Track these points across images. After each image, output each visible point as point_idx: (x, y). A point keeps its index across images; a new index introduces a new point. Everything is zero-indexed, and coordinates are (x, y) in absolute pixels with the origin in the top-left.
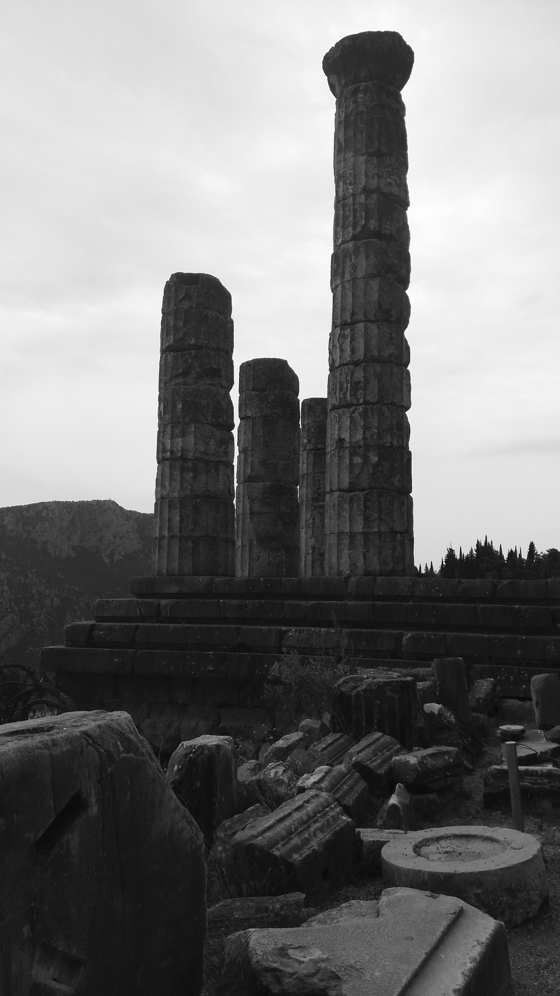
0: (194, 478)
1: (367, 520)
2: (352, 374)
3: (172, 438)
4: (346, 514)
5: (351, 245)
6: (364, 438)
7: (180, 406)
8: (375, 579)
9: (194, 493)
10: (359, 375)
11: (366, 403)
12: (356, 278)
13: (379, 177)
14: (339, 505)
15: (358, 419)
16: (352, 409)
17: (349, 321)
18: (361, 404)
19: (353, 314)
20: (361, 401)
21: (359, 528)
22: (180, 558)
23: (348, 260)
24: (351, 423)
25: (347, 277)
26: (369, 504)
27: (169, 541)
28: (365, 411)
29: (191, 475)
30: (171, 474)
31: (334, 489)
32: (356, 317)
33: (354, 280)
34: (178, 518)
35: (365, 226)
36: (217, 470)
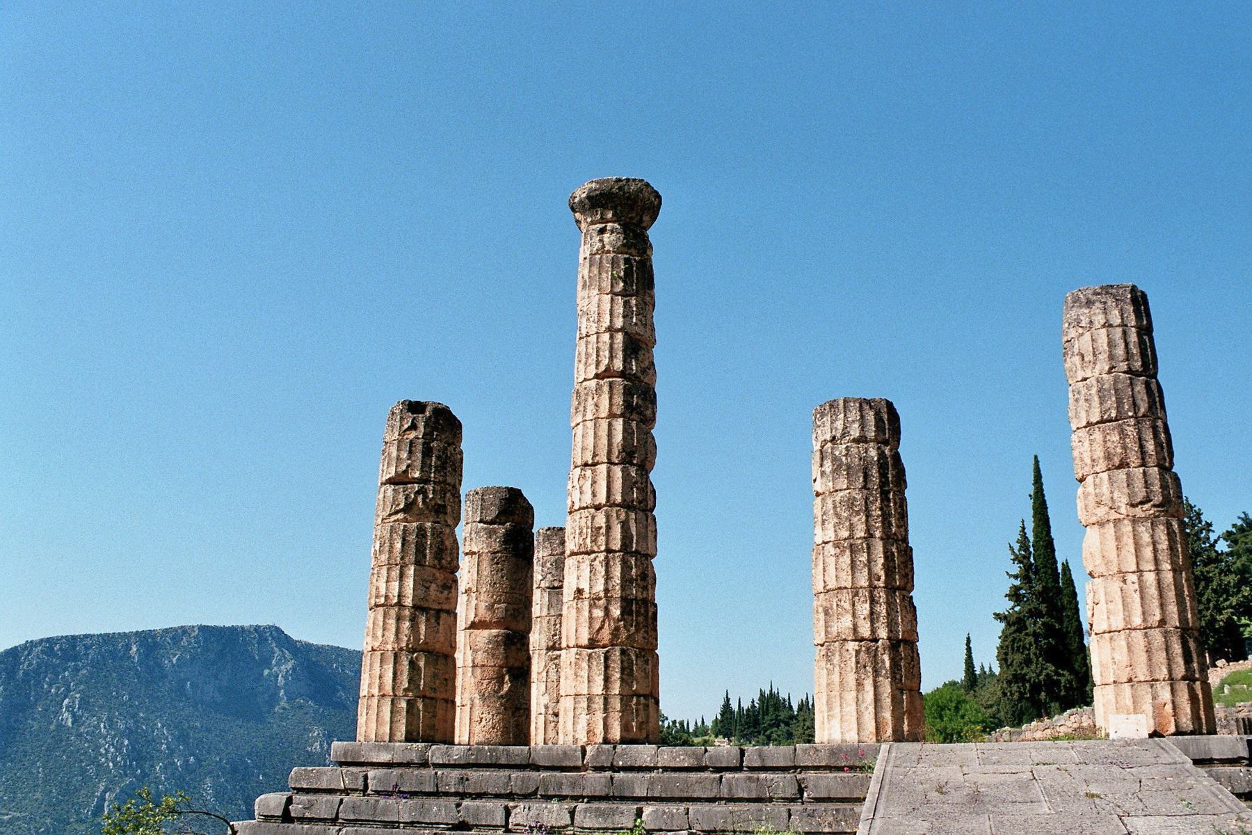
2: (593, 518)
4: (584, 673)
5: (593, 383)
6: (606, 590)
8: (615, 748)
10: (601, 520)
11: (608, 551)
16: (593, 556)
17: (590, 462)
19: (595, 455)
28: (606, 557)
36: (438, 618)
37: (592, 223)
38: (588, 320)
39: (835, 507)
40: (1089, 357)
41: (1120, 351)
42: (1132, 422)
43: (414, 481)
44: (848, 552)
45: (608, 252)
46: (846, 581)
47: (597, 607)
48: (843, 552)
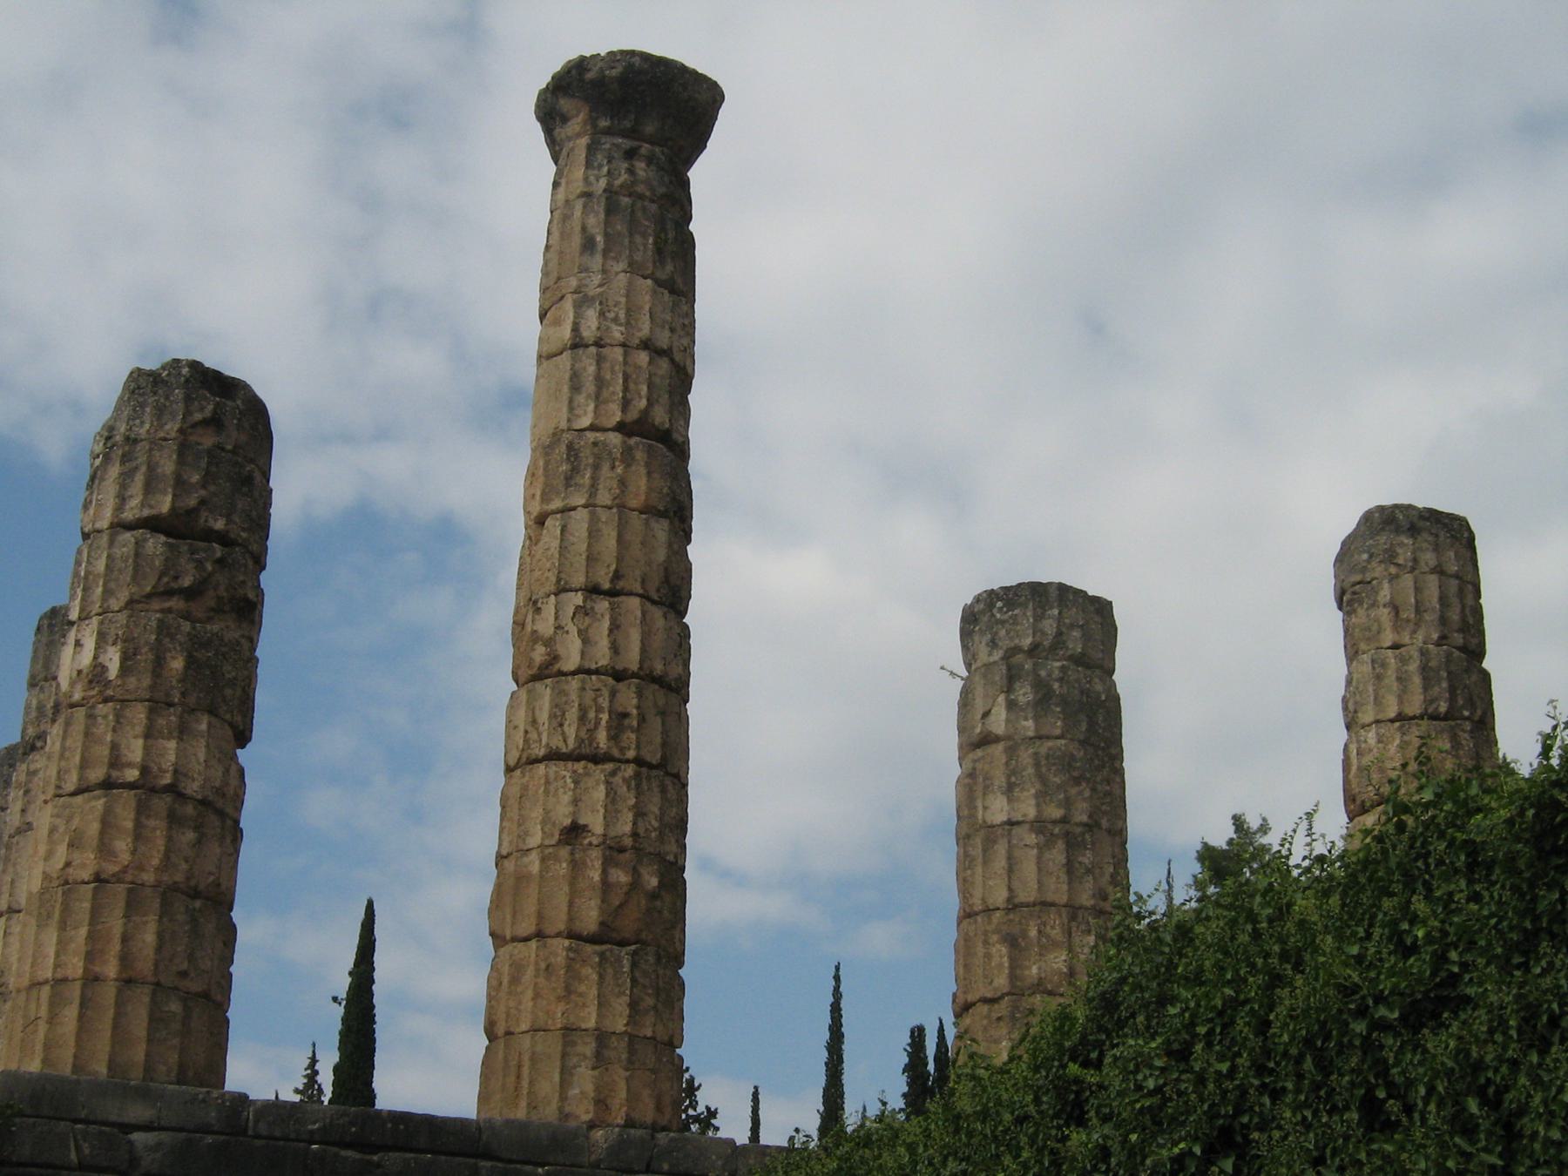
0: (199, 842)
3: (147, 736)
6: (635, 835)
7: (177, 664)
9: (193, 883)
13: (672, 330)
14: (569, 968)
16: (609, 766)
17: (606, 586)
18: (628, 761)
19: (617, 576)
20: (631, 754)
21: (620, 1025)
22: (150, 1041)
24: (607, 795)
25: (604, 497)
26: (637, 974)
27: (120, 992)
28: (637, 775)
29: (190, 836)
30: (138, 825)
31: (550, 929)
35: (646, 413)
37: (608, 132)
38: (602, 314)
39: (1037, 765)
40: (1408, 613)
41: (1454, 616)
42: (1468, 726)
43: (209, 535)
44: (1061, 845)
45: (641, 197)
46: (1058, 891)
47: (617, 865)
48: (1048, 844)
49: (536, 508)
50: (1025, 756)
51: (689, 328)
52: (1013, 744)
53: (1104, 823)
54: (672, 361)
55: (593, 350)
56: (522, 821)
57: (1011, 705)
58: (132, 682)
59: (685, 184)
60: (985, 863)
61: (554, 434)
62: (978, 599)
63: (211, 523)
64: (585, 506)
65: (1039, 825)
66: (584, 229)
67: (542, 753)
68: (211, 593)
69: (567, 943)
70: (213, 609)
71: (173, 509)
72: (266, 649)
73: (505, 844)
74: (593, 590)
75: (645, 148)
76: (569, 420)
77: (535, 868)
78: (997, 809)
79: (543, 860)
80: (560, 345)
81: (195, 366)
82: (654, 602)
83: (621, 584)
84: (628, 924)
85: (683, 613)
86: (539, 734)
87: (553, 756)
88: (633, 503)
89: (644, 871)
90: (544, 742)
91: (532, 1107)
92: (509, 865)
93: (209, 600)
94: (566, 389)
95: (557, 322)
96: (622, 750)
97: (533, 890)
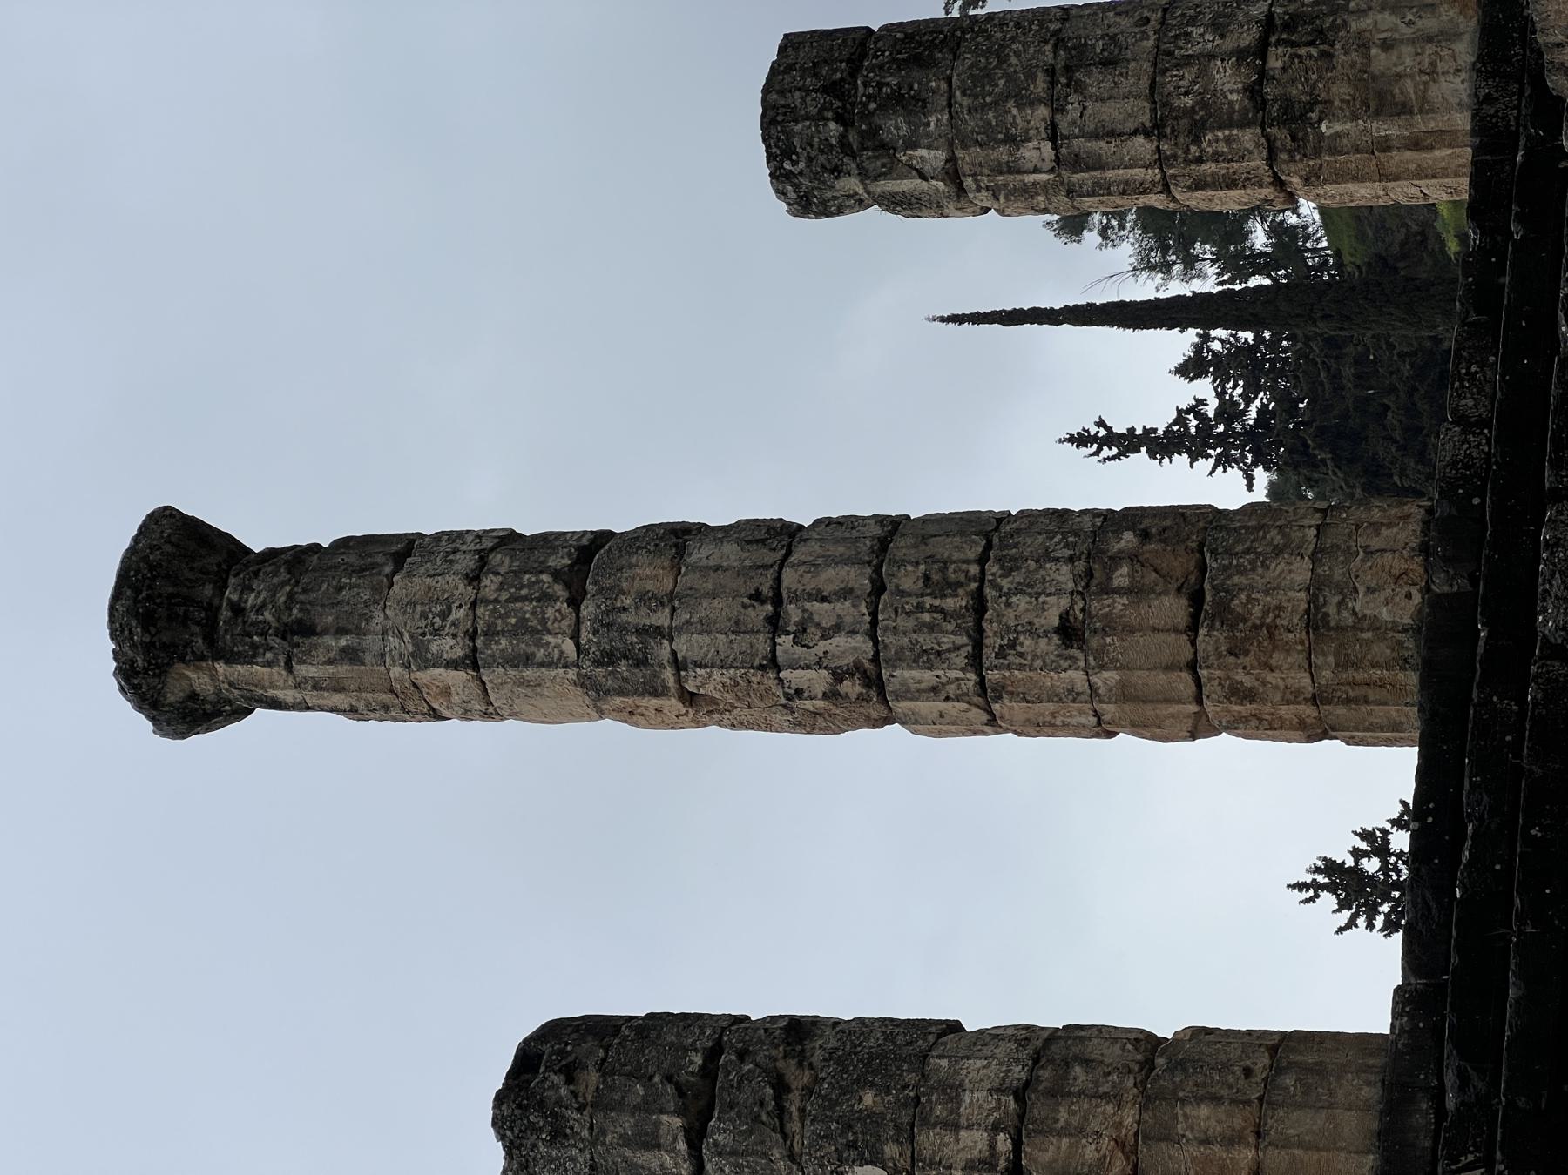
0: (1086, 1062)
1: (1278, 551)
2: (902, 593)
6: (1071, 559)
12: (672, 593)
15: (1018, 577)
16: (990, 593)
17: (769, 608)
18: (983, 572)
19: (757, 597)
20: (974, 569)
23: (624, 617)
24: (1023, 592)
25: (661, 618)
26: (1239, 548)
29: (1078, 1070)
32: (766, 590)
33: (670, 600)
34: (1204, 1111)
35: (556, 575)
37: (210, 639)
38: (436, 633)
39: (985, 107)
43: (709, 1071)
45: (291, 596)
46: (1135, 78)
48: (1079, 87)
49: (672, 704)
50: (971, 123)
51: (452, 540)
52: (955, 140)
53: (1053, 27)
54: (492, 550)
55: (479, 642)
56: (1054, 697)
57: (912, 144)
58: (891, 1150)
59: (271, 554)
60: (1101, 166)
61: (582, 686)
62: (781, 194)
63: (694, 1068)
64: (671, 640)
65: (1057, 106)
66: (330, 662)
67: (972, 676)
68: (780, 1064)
69: (1202, 632)
70: (800, 1064)
71: (678, 1113)
72: (845, 1010)
73: (1083, 720)
74: (775, 624)
75: (231, 594)
76: (566, 666)
77: (1112, 676)
78: (1037, 152)
79: (1103, 667)
80: (474, 684)
81: (500, 1099)
82: (788, 554)
83: (766, 590)
84: (1180, 564)
85: (801, 527)
86: (950, 682)
87: (976, 661)
88: (668, 583)
89: (1116, 547)
90: (960, 675)
91: (1405, 663)
92: (1109, 710)
93: (790, 1069)
94: (528, 673)
95: (446, 691)
96: (969, 579)
97: (1139, 677)
